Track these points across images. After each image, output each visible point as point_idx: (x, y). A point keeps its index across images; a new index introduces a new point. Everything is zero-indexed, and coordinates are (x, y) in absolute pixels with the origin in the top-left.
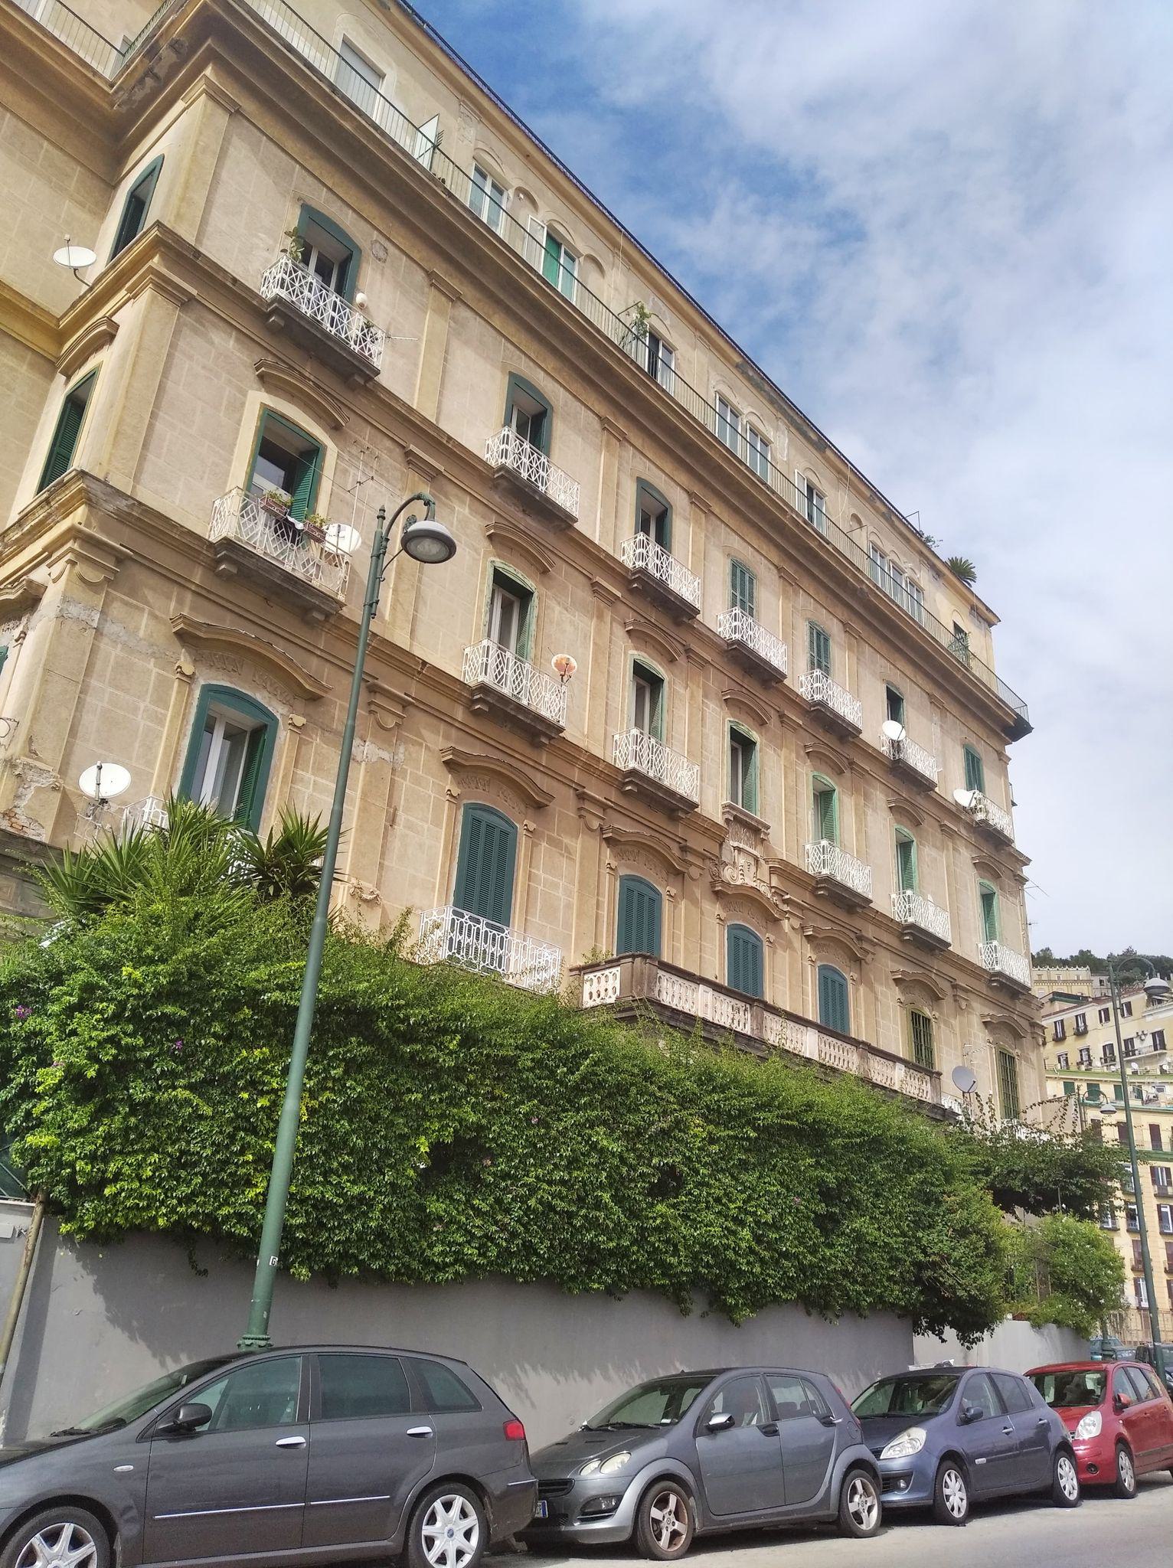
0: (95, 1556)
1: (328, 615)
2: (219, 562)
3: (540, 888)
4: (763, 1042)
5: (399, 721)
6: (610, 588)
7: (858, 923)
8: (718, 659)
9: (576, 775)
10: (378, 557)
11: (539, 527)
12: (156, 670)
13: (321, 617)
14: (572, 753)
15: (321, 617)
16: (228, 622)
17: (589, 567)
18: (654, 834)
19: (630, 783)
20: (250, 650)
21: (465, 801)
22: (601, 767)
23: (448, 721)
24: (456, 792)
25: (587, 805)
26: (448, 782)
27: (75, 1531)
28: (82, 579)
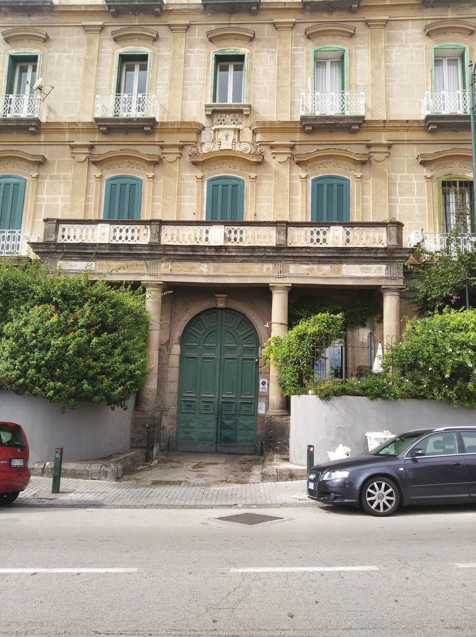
0: (394, 502)
1: (360, 125)
2: (428, 127)
3: (398, 205)
4: (160, 246)
5: (388, 155)
6: (285, 20)
7: (364, 136)
8: (301, 16)
9: (67, 137)
10: (472, 85)
11: (40, 18)
12: (416, 182)
13: (357, 127)
14: (56, 128)
15: (357, 127)
16: (441, 148)
17: (72, 20)
18: (122, 147)
19: (430, 124)
20: (218, 157)
21: (208, 178)
22: (80, 126)
23: (410, 142)
24: (429, 175)
25: (75, 151)
26: (425, 172)
27: (392, 492)
28: (280, 162)
